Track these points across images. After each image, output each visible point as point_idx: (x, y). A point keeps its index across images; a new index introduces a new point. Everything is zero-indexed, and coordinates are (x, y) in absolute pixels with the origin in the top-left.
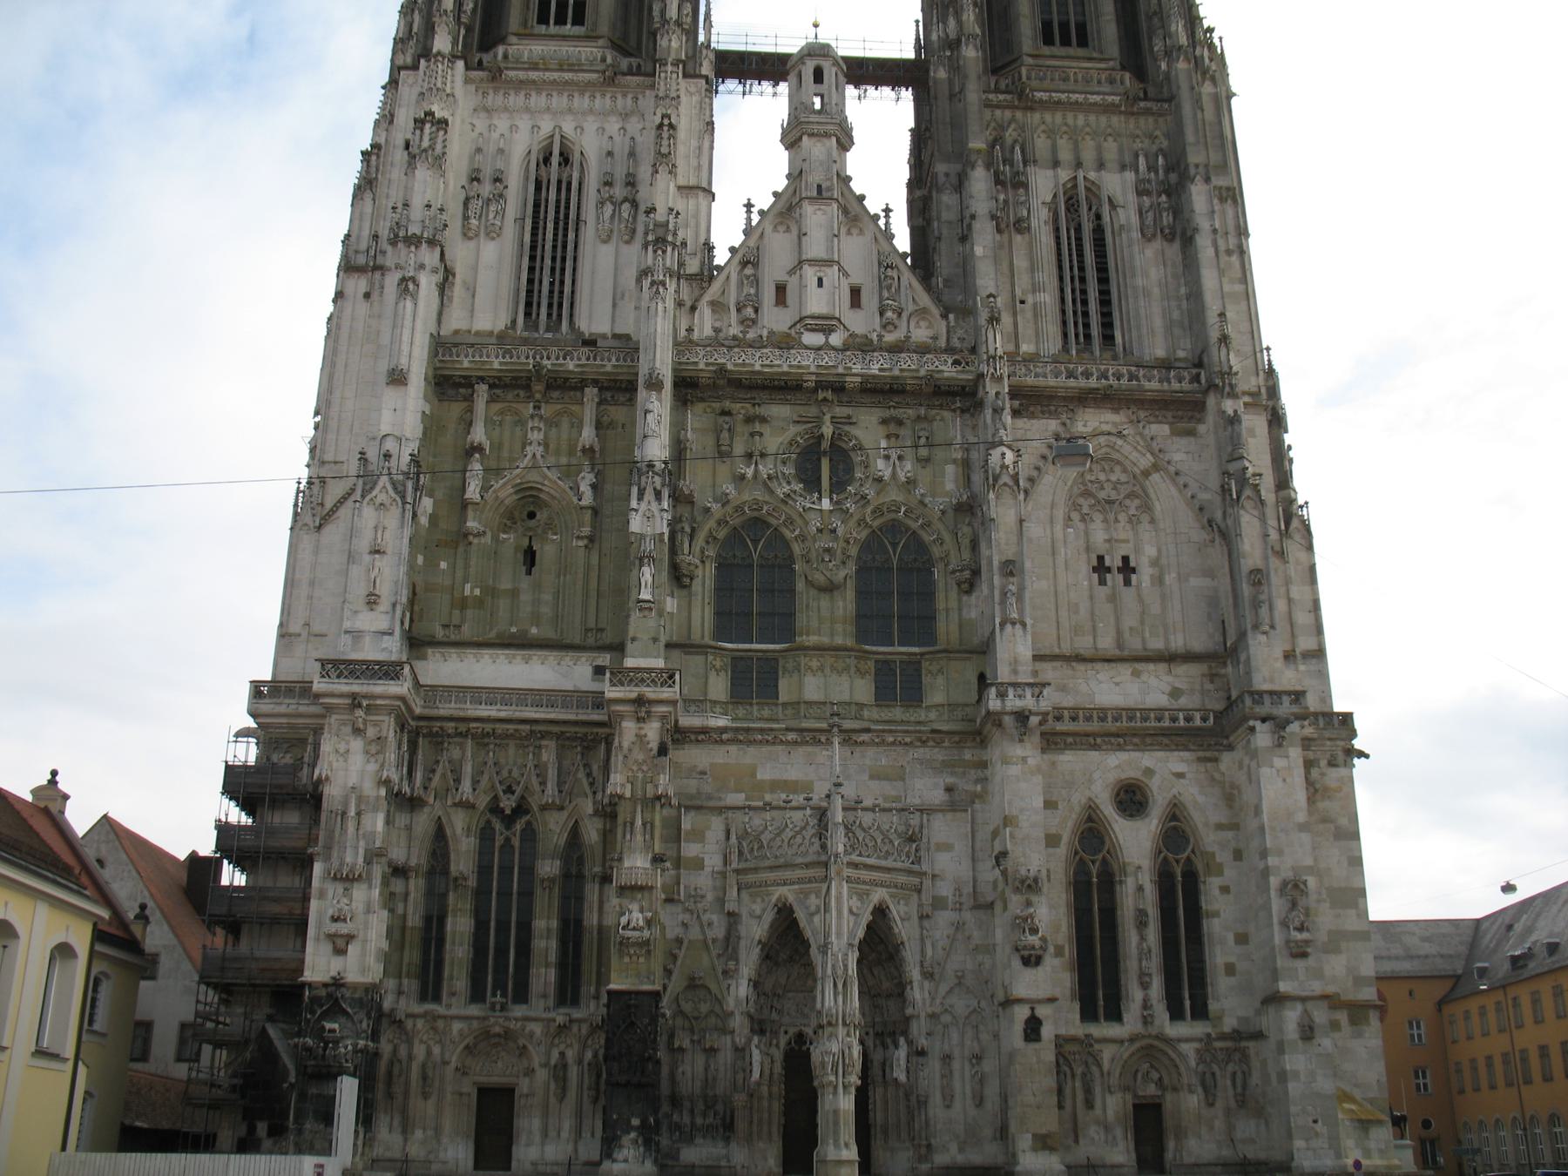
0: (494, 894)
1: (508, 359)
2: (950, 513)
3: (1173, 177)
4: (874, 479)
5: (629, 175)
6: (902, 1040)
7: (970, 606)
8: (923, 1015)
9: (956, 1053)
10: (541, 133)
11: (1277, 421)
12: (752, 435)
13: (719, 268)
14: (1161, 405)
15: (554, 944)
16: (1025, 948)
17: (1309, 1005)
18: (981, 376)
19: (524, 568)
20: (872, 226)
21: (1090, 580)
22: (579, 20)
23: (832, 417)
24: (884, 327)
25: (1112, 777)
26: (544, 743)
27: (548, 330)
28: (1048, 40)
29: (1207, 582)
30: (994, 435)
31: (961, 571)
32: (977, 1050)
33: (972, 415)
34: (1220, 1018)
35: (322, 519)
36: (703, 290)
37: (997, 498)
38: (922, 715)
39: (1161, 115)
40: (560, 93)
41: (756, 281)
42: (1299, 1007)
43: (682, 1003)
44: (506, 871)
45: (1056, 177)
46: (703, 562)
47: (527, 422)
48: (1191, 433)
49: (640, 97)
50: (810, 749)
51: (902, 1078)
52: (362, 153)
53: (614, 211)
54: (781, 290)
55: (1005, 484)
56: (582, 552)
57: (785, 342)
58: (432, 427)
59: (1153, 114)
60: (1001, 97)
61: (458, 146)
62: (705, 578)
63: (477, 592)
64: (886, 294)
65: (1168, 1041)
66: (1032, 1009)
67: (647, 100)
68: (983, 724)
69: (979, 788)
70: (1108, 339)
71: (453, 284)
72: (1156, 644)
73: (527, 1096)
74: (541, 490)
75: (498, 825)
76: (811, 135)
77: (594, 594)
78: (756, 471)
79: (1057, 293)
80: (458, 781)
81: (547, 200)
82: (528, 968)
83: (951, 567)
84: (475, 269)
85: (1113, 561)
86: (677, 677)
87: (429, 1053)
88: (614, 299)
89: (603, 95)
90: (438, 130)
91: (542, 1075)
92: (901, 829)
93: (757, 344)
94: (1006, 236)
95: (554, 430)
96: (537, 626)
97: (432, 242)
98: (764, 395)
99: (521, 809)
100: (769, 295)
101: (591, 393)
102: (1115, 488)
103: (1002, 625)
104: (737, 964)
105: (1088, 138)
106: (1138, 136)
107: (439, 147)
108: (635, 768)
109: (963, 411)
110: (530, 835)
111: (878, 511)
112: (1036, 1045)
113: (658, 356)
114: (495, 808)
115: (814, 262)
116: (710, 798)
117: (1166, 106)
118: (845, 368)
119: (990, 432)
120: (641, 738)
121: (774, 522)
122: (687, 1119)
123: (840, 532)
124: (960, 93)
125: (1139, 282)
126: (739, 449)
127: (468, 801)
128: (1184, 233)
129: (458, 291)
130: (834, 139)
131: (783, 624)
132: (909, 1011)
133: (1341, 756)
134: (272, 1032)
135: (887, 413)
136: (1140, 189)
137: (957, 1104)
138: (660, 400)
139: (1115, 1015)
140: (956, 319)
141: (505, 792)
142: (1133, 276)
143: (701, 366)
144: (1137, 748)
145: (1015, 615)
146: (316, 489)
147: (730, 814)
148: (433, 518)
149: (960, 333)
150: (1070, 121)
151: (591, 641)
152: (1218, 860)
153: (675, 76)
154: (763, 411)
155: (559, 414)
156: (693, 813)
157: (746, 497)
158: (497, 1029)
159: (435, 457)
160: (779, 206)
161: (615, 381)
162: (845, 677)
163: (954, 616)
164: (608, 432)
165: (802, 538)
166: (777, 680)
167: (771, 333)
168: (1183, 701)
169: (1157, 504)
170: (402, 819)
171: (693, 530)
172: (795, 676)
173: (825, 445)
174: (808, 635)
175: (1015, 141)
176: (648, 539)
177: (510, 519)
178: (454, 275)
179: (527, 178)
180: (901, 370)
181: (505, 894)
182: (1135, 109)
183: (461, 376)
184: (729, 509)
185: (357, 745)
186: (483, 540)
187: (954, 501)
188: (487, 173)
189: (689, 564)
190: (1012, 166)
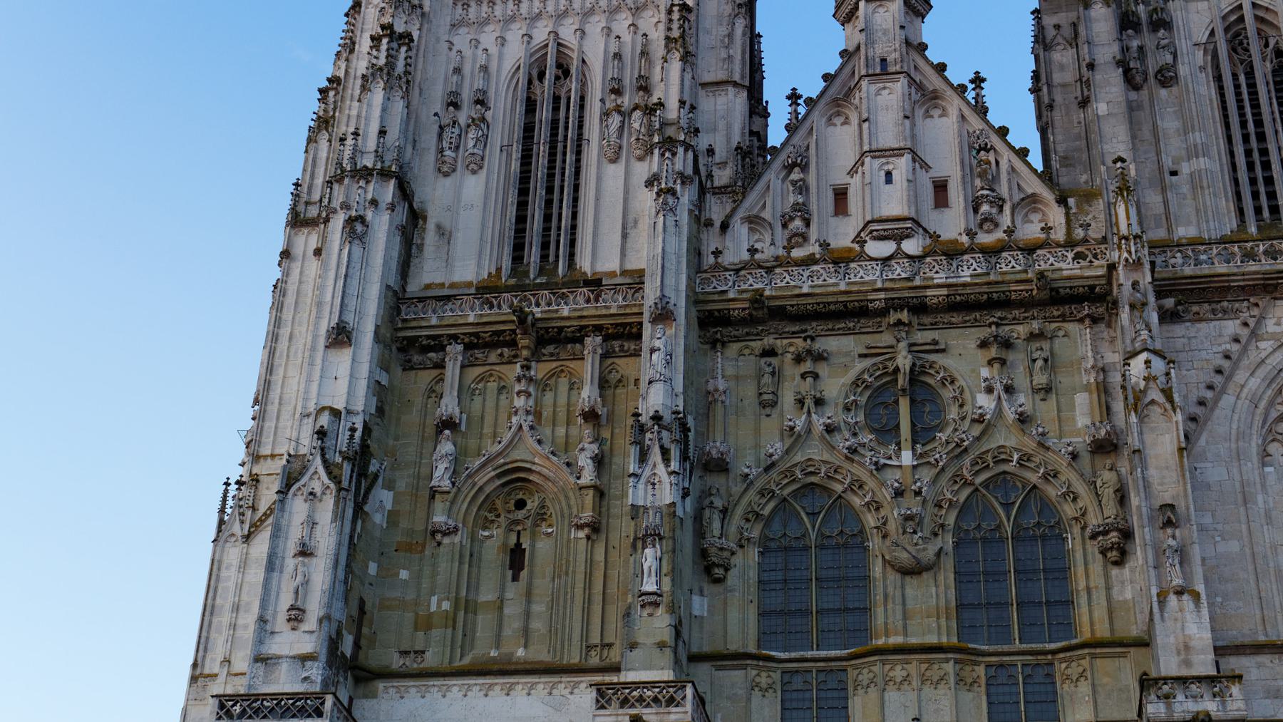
2: (1086, 459)
4: (974, 421)
7: (1123, 583)
10: (532, 45)
12: (803, 376)
19: (509, 573)
31: (1105, 533)
33: (1109, 326)
36: (737, 204)
41: (802, 188)
47: (512, 387)
53: (623, 122)
55: (1153, 402)
62: (746, 564)
63: (446, 605)
64: (978, 182)
71: (424, 230)
74: (529, 470)
77: (598, 598)
79: (1225, 159)
88: (624, 228)
90: (400, 46)
94: (1144, 93)
97: (385, 174)
107: (400, 67)
109: (1095, 320)
111: (980, 464)
115: (878, 153)
121: (839, 488)
126: (788, 399)
135: (985, 333)
148: (393, 517)
151: (594, 660)
154: (822, 344)
155: (554, 374)
157: (799, 458)
161: (624, 325)
163: (1100, 598)
164: (618, 391)
172: (872, 689)
173: (902, 381)
174: (887, 635)
177: (487, 510)
178: (425, 219)
183: (428, 337)
184: (774, 474)
186: (457, 539)
188: (466, 96)
189: (722, 549)
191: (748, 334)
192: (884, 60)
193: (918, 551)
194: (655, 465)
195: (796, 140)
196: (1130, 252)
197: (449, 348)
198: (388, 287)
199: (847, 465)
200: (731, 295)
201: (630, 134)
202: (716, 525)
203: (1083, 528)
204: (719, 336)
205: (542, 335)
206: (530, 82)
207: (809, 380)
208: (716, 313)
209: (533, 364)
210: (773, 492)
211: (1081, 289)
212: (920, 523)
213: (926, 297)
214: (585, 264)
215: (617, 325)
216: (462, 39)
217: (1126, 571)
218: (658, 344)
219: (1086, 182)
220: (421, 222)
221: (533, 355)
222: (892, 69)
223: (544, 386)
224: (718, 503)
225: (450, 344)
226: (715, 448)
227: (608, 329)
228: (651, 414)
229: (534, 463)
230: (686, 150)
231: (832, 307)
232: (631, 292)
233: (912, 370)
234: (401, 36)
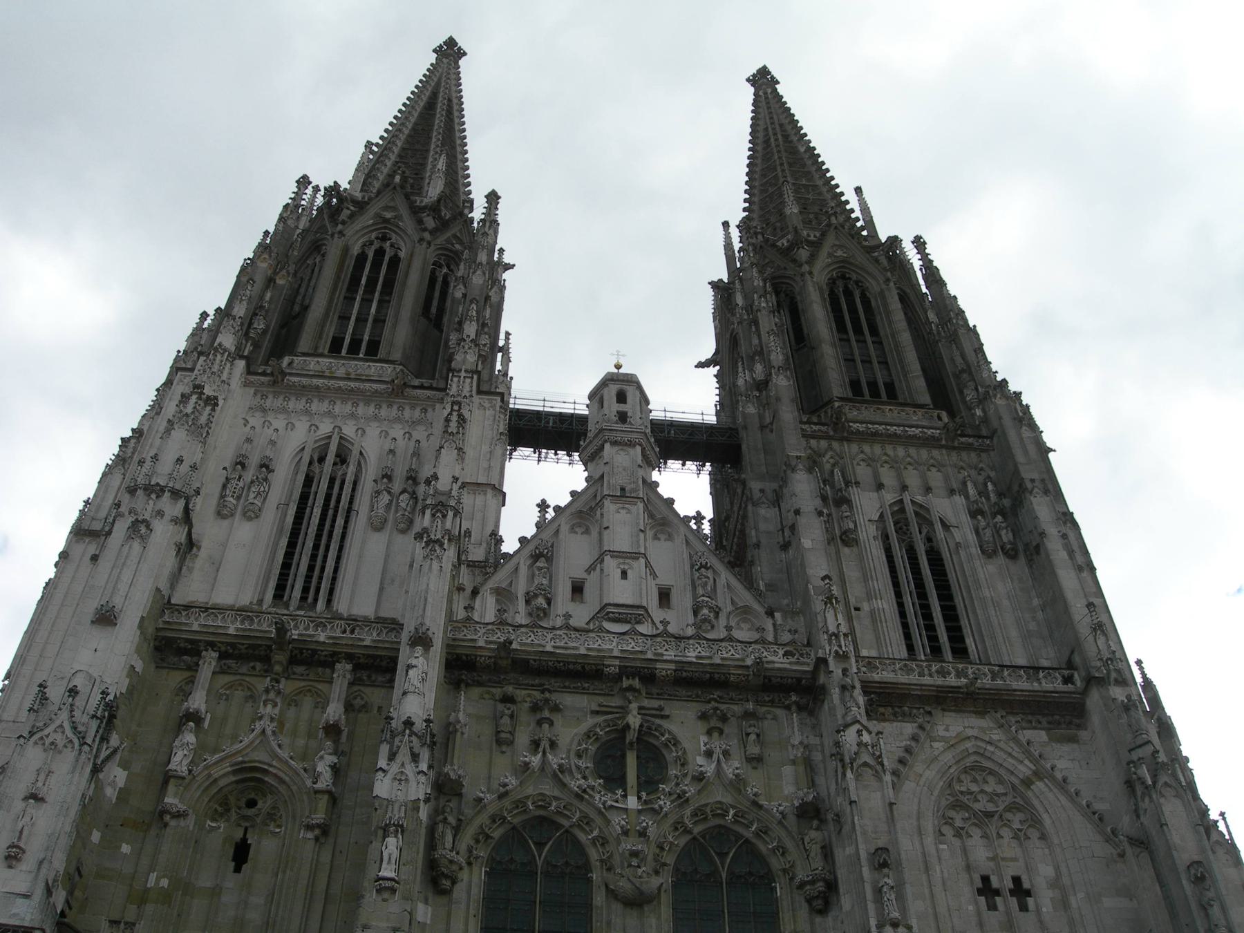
2: (792, 820)
3: (1006, 502)
4: (694, 778)
5: (411, 469)
10: (317, 434)
12: (539, 723)
13: (507, 556)
20: (682, 529)
21: (976, 903)
23: (640, 708)
36: (487, 576)
37: (857, 779)
39: (983, 451)
40: (344, 401)
46: (469, 864)
48: (1073, 740)
49: (430, 410)
52: (123, 439)
53: (391, 501)
55: (865, 764)
59: (975, 450)
63: (165, 883)
71: (197, 556)
74: (265, 771)
78: (544, 762)
83: (797, 880)
84: (224, 545)
88: (382, 583)
89: (390, 406)
95: (293, 709)
97: (176, 494)
98: (555, 683)
100: (563, 590)
101: (343, 669)
105: (910, 468)
106: (962, 468)
107: (203, 419)
109: (801, 708)
111: (700, 814)
113: (428, 613)
115: (616, 554)
118: (655, 654)
121: (566, 823)
123: (652, 832)
124: (771, 423)
126: (523, 738)
130: (639, 449)
138: (427, 659)
140: (784, 617)
148: (124, 794)
150: (890, 452)
153: (468, 381)
154: (555, 697)
155: (300, 692)
157: (530, 790)
159: (139, 725)
161: (374, 657)
164: (360, 715)
165: (602, 841)
169: (1045, 816)
173: (631, 736)
175: (833, 465)
176: (396, 806)
178: (199, 548)
179: (296, 473)
180: (723, 659)
182: (956, 444)
183: (187, 640)
184: (507, 803)
186: (182, 823)
188: (254, 461)
189: (451, 862)
191: (489, 680)
192: (623, 489)
193: (642, 883)
194: (403, 765)
196: (840, 646)
197: (204, 653)
198: (158, 590)
199: (576, 802)
200: (481, 643)
201: (396, 511)
203: (792, 879)
204: (463, 677)
205: (296, 655)
206: (311, 463)
207: (546, 726)
208: (464, 657)
209: (283, 680)
210: (505, 818)
211: (790, 680)
212: (644, 860)
213: (656, 669)
214: (342, 605)
215: (369, 656)
216: (255, 421)
217: (830, 919)
218: (414, 662)
219: (788, 605)
220: (195, 549)
221: (284, 671)
223: (293, 701)
224: (452, 820)
225: (207, 650)
226: (453, 771)
227: (359, 658)
228: (404, 718)
229: (271, 766)
230: (455, 515)
231: (571, 667)
232: (385, 631)
233: (640, 731)
234: (208, 398)
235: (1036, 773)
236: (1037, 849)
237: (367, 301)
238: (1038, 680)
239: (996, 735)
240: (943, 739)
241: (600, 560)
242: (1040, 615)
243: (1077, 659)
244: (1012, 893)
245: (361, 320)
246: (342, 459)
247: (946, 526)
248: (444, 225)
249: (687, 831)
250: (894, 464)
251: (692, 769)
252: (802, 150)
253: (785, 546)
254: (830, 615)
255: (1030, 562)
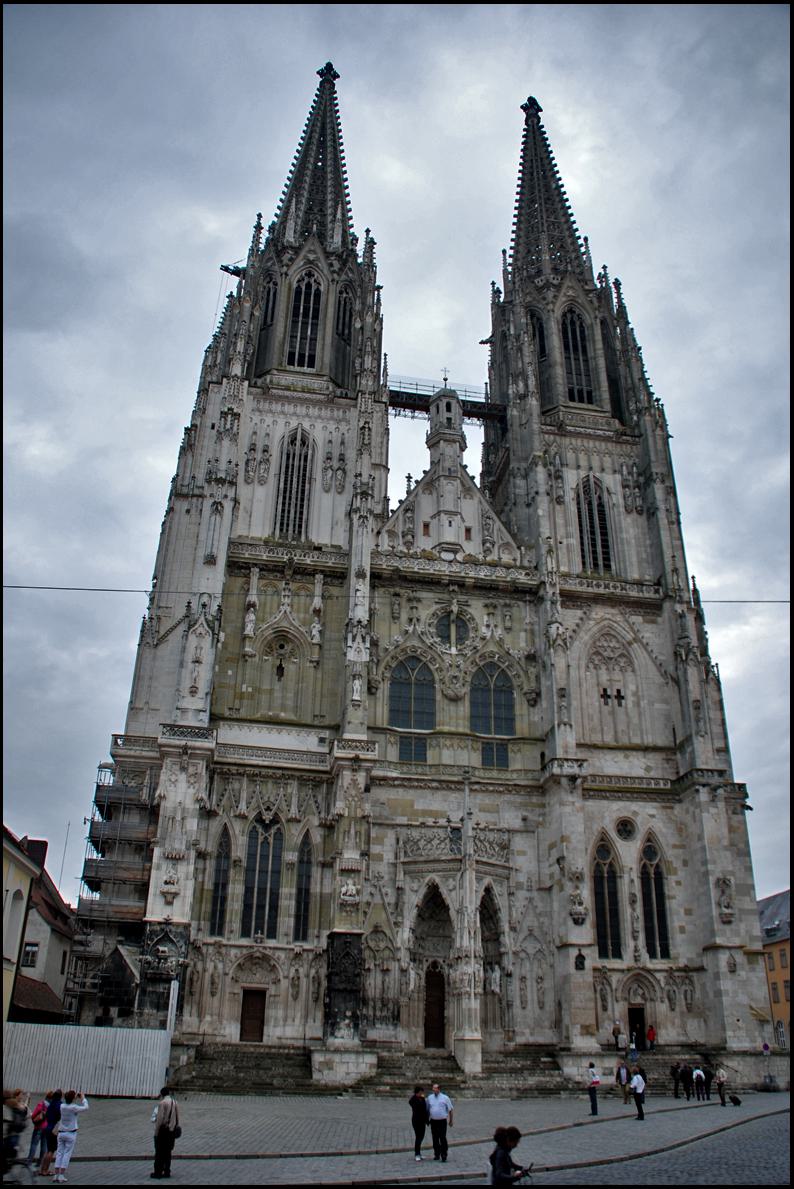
0: (257, 872)
1: (271, 554)
2: (523, 659)
5: (341, 455)
6: (497, 967)
8: (510, 952)
9: (528, 977)
10: (291, 426)
11: (700, 618)
12: (412, 608)
14: (639, 605)
15: (293, 903)
16: (576, 914)
17: (733, 952)
18: (543, 583)
21: (600, 702)
22: (311, 364)
24: (484, 552)
25: (615, 816)
26: (289, 781)
27: (293, 539)
28: (572, 399)
29: (664, 706)
30: (552, 616)
32: (541, 974)
33: (535, 605)
34: (676, 958)
35: (159, 640)
38: (508, 776)
39: (634, 445)
40: (302, 405)
42: (727, 953)
43: (369, 941)
44: (264, 857)
45: (578, 474)
48: (653, 622)
50: (445, 792)
51: (497, 990)
54: (426, 526)
56: (312, 670)
57: (428, 557)
58: (226, 592)
60: (549, 428)
61: (245, 429)
62: (384, 689)
63: (250, 690)
64: (486, 533)
65: (649, 971)
66: (580, 950)
67: (353, 414)
68: (546, 781)
69: (541, 819)
70: (607, 567)
72: (636, 741)
73: (275, 996)
74: (288, 632)
75: (260, 830)
76: (445, 441)
77: (319, 695)
78: (415, 629)
80: (238, 802)
81: (293, 465)
82: (276, 917)
85: (612, 692)
86: (377, 746)
87: (215, 967)
89: (326, 409)
91: (285, 983)
92: (499, 842)
93: (414, 556)
96: (285, 712)
99: (275, 820)
100: (420, 529)
101: (319, 577)
102: (612, 651)
103: (559, 725)
104: (403, 919)
107: (235, 428)
108: (350, 799)
110: (279, 836)
111: (482, 657)
112: (582, 972)
114: (259, 819)
115: (447, 512)
116: (387, 818)
117: (637, 439)
119: (550, 615)
120: (354, 781)
122: (371, 1013)
123: (462, 666)
125: (624, 536)
126: (404, 617)
127: (244, 814)
128: (648, 510)
129: (241, 513)
131: (428, 717)
132: (502, 950)
133: (739, 808)
134: (123, 950)
135: (488, 601)
136: (625, 483)
137: (529, 1007)
139: (618, 955)
140: (526, 549)
141: (266, 810)
142: (621, 532)
143: (384, 567)
144: (628, 799)
145: (566, 720)
146: (154, 622)
147: (399, 829)
149: (528, 558)
150: (586, 444)
152: (674, 865)
154: (419, 594)
156: (377, 827)
157: (408, 644)
158: (258, 954)
160: (425, 480)
162: (465, 751)
163: (526, 719)
166: (426, 750)
167: (424, 550)
168: (652, 774)
170: (204, 824)
171: (378, 661)
172: (437, 748)
173: (453, 617)
177: (269, 649)
181: (263, 871)
182: (621, 440)
184: (398, 650)
185: (183, 777)
187: (526, 653)
188: (260, 447)
190: (554, 466)
195: (411, 499)
202: (375, 670)
203: (522, 689)
207: (414, 610)
216: (256, 418)
217: (536, 709)
218: (359, 588)
222: (453, 475)
224: (375, 660)
228: (357, 619)
235: (634, 639)
236: (630, 676)
237: (305, 324)
238: (642, 591)
239: (619, 618)
240: (594, 619)
241: (439, 513)
242: (649, 550)
243: (663, 582)
244: (616, 697)
245: (303, 338)
246: (303, 443)
247: (609, 493)
248: (344, 263)
249: (477, 664)
250: (587, 451)
251: (480, 634)
252: (554, 186)
253: (528, 505)
254: (549, 559)
255: (648, 519)
